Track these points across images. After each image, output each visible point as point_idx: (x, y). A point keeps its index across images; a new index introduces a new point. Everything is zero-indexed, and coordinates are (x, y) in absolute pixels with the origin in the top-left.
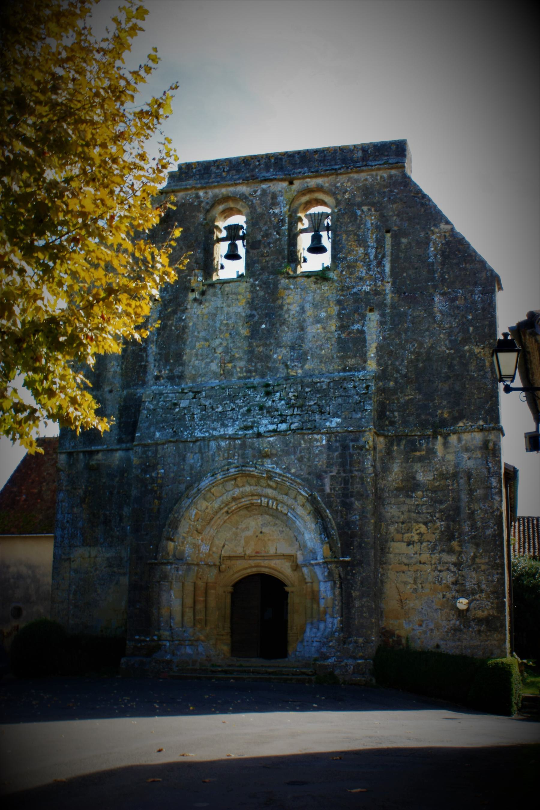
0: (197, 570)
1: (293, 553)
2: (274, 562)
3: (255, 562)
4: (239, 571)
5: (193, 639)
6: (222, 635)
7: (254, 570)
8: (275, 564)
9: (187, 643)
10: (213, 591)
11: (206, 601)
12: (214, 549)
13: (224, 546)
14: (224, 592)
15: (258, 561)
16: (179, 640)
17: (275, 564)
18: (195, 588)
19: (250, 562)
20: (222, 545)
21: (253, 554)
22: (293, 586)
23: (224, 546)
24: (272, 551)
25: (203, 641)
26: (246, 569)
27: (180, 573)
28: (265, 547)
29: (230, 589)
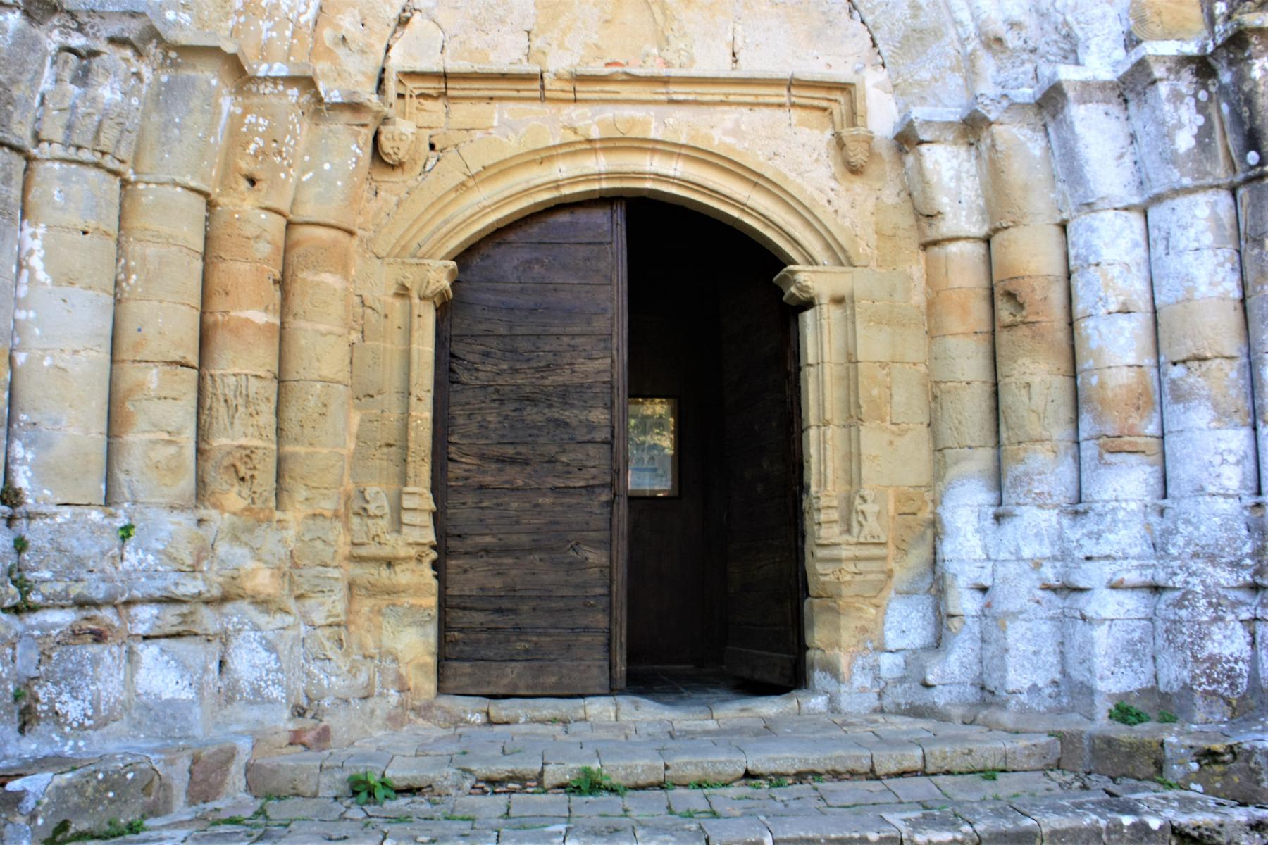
0: (235, 122)
1: (841, 73)
2: (729, 117)
3: (609, 112)
4: (502, 168)
5: (190, 587)
6: (390, 563)
7: (600, 163)
8: (736, 132)
9: (145, 616)
10: (330, 279)
11: (282, 335)
12: (348, 23)
13: (403, 22)
14: (403, 292)
15: (627, 112)
16: (82, 603)
17: (736, 132)
18: (207, 239)
19: (573, 113)
20: (393, 13)
21: (598, 68)
22: (841, 257)
23: (403, 22)
24: (713, 62)
25: (263, 603)
26: (545, 156)
27: (107, 92)
28: (663, 41)
29: (439, 275)
